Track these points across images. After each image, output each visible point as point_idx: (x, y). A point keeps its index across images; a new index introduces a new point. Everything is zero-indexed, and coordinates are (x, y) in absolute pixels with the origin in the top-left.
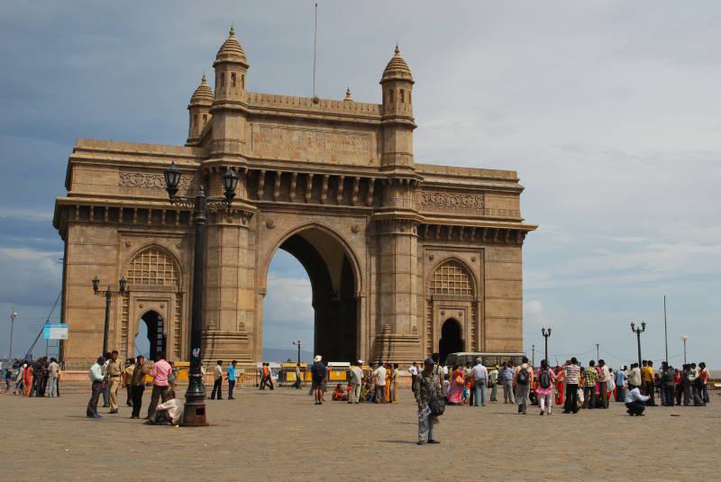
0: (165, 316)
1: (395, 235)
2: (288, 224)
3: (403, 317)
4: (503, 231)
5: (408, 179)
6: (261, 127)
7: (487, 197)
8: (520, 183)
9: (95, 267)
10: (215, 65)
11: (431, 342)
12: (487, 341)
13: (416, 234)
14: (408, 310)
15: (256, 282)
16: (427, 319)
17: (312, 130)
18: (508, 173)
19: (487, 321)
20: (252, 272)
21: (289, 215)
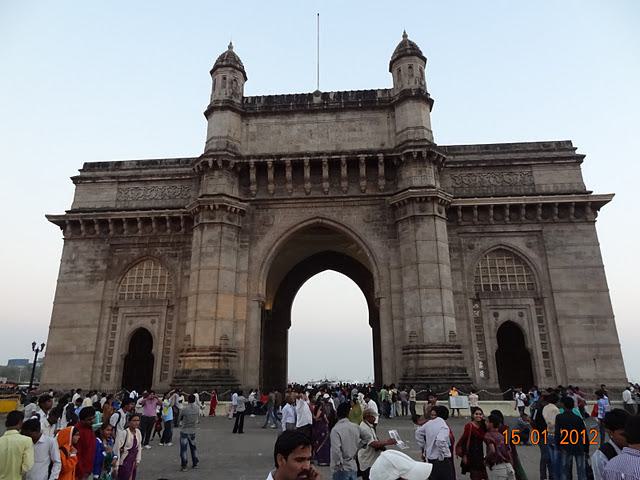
0: (156, 331)
1: (414, 218)
2: (285, 220)
3: (433, 319)
4: (564, 206)
5: (424, 151)
6: (258, 125)
7: (536, 172)
8: (577, 152)
9: (83, 283)
10: (212, 72)
11: (483, 353)
12: (565, 350)
13: (444, 215)
14: (439, 310)
15: (249, 287)
16: (473, 325)
17: (313, 122)
18: (559, 143)
19: (561, 323)
20: (244, 276)
21: (287, 210)
